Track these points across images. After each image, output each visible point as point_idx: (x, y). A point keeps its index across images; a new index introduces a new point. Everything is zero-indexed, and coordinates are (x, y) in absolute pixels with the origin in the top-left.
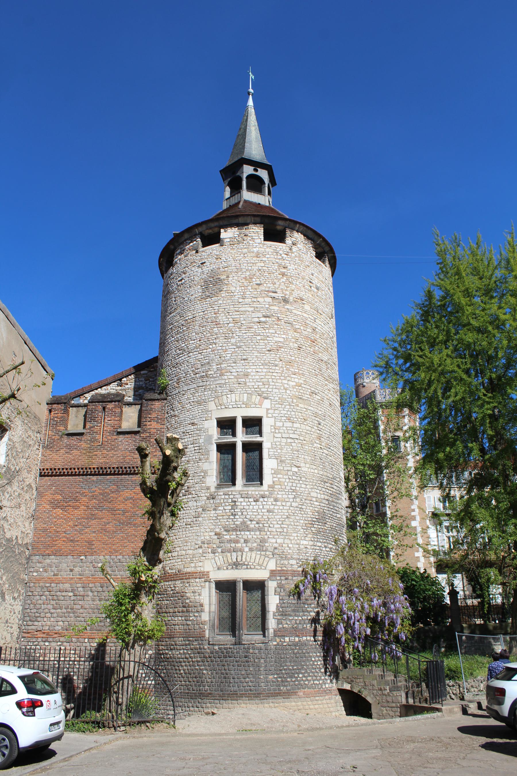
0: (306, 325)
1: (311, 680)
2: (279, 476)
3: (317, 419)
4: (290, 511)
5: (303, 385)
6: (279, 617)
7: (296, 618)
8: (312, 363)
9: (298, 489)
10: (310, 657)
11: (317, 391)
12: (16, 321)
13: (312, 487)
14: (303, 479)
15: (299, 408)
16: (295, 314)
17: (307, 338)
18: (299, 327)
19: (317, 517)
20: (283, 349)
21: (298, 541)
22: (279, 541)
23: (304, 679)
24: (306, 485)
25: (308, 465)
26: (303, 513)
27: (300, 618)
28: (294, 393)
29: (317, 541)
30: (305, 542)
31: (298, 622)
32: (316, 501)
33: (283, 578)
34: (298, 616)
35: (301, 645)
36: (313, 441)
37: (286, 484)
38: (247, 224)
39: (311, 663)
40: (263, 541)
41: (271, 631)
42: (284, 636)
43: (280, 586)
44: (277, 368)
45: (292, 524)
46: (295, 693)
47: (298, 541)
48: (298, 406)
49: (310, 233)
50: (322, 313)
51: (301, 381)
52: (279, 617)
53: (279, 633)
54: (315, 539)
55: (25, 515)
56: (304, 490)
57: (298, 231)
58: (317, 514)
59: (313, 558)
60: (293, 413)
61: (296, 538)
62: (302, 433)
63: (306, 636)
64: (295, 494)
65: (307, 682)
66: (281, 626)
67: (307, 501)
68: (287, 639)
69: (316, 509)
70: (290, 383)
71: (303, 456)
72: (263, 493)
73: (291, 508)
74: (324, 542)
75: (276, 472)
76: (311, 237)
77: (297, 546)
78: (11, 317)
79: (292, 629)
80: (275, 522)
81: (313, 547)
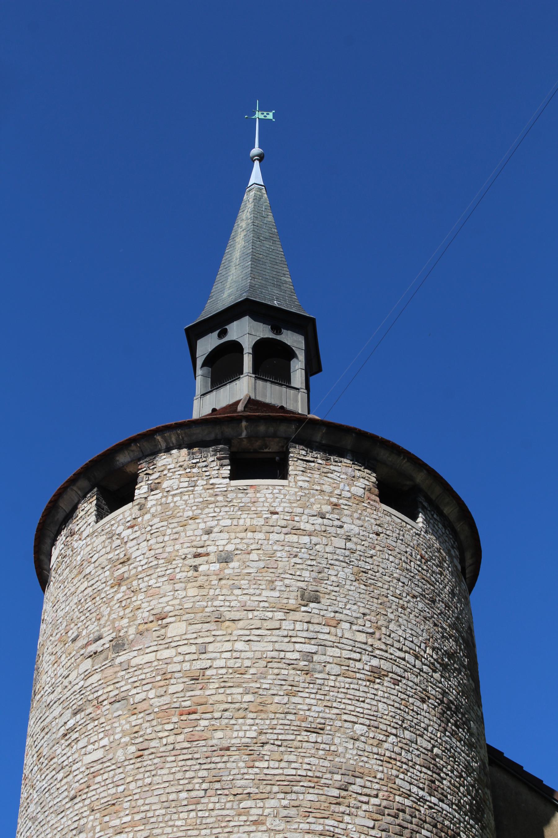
0: (166, 677)
8: (179, 776)
16: (139, 667)
17: (166, 710)
20: (99, 779)
38: (75, 508)
50: (237, 615)
57: (168, 450)
76: (212, 436)
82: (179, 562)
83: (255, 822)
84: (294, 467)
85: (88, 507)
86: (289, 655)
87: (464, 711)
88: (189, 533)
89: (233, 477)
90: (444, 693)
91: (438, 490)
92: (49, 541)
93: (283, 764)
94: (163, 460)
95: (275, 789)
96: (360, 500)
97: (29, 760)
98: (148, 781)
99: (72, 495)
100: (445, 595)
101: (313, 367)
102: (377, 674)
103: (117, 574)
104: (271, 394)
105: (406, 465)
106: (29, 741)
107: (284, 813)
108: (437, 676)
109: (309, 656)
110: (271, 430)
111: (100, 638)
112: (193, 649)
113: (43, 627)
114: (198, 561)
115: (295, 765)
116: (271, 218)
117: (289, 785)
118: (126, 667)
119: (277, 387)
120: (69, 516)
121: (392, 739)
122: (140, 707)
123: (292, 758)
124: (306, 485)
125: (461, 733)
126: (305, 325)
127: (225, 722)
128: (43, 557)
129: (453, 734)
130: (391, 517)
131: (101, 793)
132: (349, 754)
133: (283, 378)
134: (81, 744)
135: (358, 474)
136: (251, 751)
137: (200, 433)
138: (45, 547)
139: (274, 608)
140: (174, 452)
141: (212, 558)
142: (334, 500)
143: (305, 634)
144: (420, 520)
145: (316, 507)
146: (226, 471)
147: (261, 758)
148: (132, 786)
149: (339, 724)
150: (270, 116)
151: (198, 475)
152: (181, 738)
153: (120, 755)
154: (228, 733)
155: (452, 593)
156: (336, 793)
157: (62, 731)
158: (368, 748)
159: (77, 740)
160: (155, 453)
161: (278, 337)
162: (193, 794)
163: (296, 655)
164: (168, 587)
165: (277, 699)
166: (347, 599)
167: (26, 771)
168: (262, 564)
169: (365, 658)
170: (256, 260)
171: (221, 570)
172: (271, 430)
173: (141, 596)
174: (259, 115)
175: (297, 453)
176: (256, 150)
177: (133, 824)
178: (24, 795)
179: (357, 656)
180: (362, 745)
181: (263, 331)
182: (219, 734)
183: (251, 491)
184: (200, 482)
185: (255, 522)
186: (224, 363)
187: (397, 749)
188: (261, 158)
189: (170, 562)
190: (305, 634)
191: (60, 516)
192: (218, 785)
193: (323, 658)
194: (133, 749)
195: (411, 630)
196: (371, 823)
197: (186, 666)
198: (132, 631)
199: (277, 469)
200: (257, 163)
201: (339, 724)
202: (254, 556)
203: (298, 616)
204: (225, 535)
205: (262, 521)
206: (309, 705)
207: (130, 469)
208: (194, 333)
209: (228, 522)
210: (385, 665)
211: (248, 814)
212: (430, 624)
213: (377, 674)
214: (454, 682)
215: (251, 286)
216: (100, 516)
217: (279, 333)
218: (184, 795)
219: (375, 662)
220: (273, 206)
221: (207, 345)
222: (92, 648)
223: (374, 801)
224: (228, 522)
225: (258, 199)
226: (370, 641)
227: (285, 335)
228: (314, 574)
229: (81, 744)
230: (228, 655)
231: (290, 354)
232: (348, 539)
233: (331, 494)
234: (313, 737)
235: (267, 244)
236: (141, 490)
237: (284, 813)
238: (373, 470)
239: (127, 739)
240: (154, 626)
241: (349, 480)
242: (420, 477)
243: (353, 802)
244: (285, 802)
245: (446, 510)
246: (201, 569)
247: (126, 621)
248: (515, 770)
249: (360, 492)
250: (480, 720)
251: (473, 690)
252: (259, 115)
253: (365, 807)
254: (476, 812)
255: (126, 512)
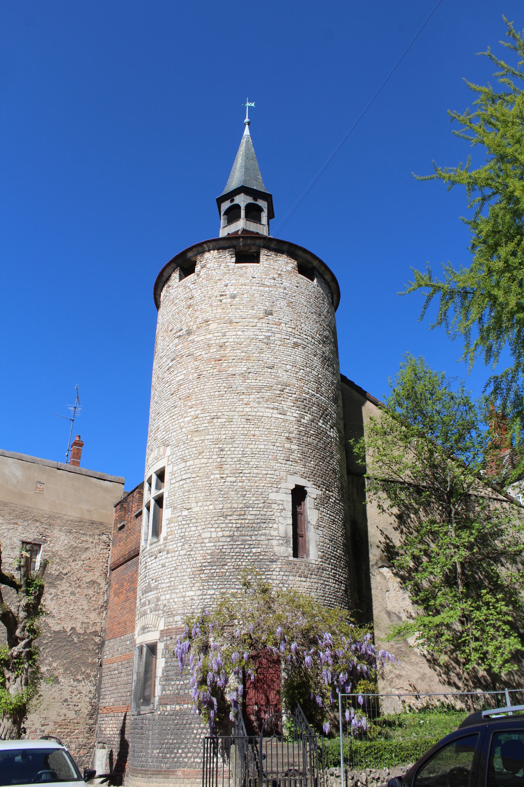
0: (209, 346)
1: (191, 757)
2: (171, 525)
3: (217, 446)
4: (177, 561)
5: (199, 416)
6: (163, 683)
7: (178, 683)
8: (215, 385)
9: (187, 534)
10: (193, 728)
11: (219, 414)
12: (33, 457)
13: (204, 527)
14: (193, 521)
15: (194, 443)
16: (198, 342)
17: (209, 360)
18: (200, 353)
19: (209, 561)
20: (182, 387)
21: (184, 593)
22: (168, 597)
23: (183, 755)
24: (197, 527)
25: (200, 504)
26: (191, 559)
27: (182, 683)
28: (188, 429)
29: (209, 589)
30: (191, 593)
31: (179, 687)
32: (210, 542)
33: (168, 638)
34: (179, 680)
35: (182, 714)
36: (210, 473)
37: (176, 532)
38: (170, 276)
39: (193, 736)
40: (158, 599)
41: (157, 699)
42: (167, 704)
43: (166, 647)
44: (176, 409)
45: (179, 575)
46: (174, 772)
47: (184, 593)
48: (192, 441)
49: (222, 244)
50: (238, 321)
51: (199, 412)
52: (163, 683)
53: (164, 701)
54: (205, 587)
55: (86, 608)
56: (194, 533)
58: (209, 557)
59: (200, 610)
60: (187, 451)
61: (182, 590)
62: (195, 469)
63: (188, 704)
64: (183, 540)
65: (186, 760)
66: (164, 692)
67: (196, 546)
68: (168, 707)
69: (209, 552)
70: (187, 419)
71: (194, 495)
72: (159, 548)
73: (179, 558)
74: (221, 588)
75: (170, 521)
76: (228, 245)
77: (182, 599)
78: (26, 456)
79: (174, 696)
80: (165, 577)
81: (201, 597)
82: (214, 298)
83: (246, 404)
84: (262, 258)
85: (176, 275)
86: (260, 337)
87: (331, 360)
88: (218, 286)
89: (237, 262)
90: (323, 353)
91: (323, 269)
92: (159, 290)
93: (257, 381)
94: (207, 255)
95: (254, 391)
96: (290, 272)
97: (154, 380)
98: (202, 387)
99: (169, 270)
100: (325, 312)
101: (271, 215)
102: (296, 345)
103: (188, 303)
104: (253, 227)
105: (309, 258)
106: (154, 372)
107: (258, 400)
108: (321, 346)
109: (268, 337)
110: (253, 242)
111: (181, 330)
112: (220, 334)
113: (158, 325)
114: (222, 298)
115: (262, 381)
116: (253, 150)
117: (259, 390)
118: (193, 341)
119: (255, 224)
120: (168, 279)
121: (302, 371)
122: (199, 358)
123: (261, 378)
124: (267, 266)
125: (330, 369)
126: (267, 197)
127: (233, 364)
128: (157, 297)
129: (327, 369)
130: (303, 279)
131: (183, 392)
132: (284, 377)
133: (257, 220)
134: (175, 373)
135: (289, 261)
136: (244, 376)
137: (222, 244)
138: (158, 292)
139: (254, 317)
140: (212, 251)
141: (228, 296)
142: (279, 272)
143: (267, 328)
144: (315, 281)
145: (272, 276)
146: (234, 260)
147: (249, 379)
148: (196, 389)
149: (280, 365)
150: (253, 105)
151: (222, 261)
152: (215, 370)
153: (191, 377)
154: (235, 368)
155: (328, 312)
156: (279, 392)
157: (167, 368)
158: (292, 375)
159: (173, 371)
160: (203, 252)
161: (256, 203)
162: (221, 393)
163: (263, 337)
164: (210, 309)
165: (255, 355)
166: (283, 313)
167: (153, 384)
168: (248, 299)
169: (291, 338)
170: (247, 169)
171: (232, 301)
172: (253, 242)
173: (198, 313)
174: (248, 104)
175: (264, 252)
176: (247, 120)
177: (196, 405)
178: (152, 393)
179: (288, 337)
180: (289, 374)
181: (249, 200)
182: (231, 369)
183: (244, 268)
184: (223, 265)
185: (246, 281)
186: (233, 214)
187: (304, 375)
188: (249, 123)
189: (210, 298)
190: (267, 328)
191: (164, 279)
192: (230, 389)
193: (274, 338)
194: (196, 375)
195: (311, 327)
196: (293, 405)
197: (217, 341)
198: (195, 327)
199: (255, 259)
200: (247, 126)
201: (280, 365)
202: (245, 296)
203: (264, 321)
204: (233, 287)
205: (249, 281)
206: (268, 357)
207: (193, 259)
208: (220, 201)
209: (234, 281)
210: (299, 341)
211: (243, 401)
212: (318, 325)
213: (296, 345)
214: (328, 348)
215: (244, 180)
216: (181, 279)
217: (256, 200)
218: (217, 393)
219: (295, 340)
220: (254, 145)
221: (226, 205)
222: (178, 334)
223: (294, 396)
224: (234, 281)
225: (247, 142)
226: (293, 331)
227: (260, 201)
228: (271, 304)
229: (175, 373)
230: (235, 337)
231: (261, 210)
232: (285, 289)
233: (278, 270)
234: (269, 370)
235: (251, 162)
236: (198, 268)
237: (258, 400)
238: (296, 259)
239: (193, 371)
240: (204, 325)
241: (285, 264)
242: (315, 263)
243: (285, 396)
244: (258, 396)
245: (326, 277)
246: (223, 301)
247: (192, 323)
248: (351, 384)
249: (290, 269)
250: (338, 364)
251: (335, 352)
252: (248, 104)
253: (290, 398)
254: (335, 400)
255: (192, 277)
